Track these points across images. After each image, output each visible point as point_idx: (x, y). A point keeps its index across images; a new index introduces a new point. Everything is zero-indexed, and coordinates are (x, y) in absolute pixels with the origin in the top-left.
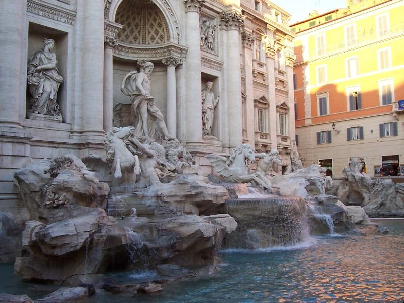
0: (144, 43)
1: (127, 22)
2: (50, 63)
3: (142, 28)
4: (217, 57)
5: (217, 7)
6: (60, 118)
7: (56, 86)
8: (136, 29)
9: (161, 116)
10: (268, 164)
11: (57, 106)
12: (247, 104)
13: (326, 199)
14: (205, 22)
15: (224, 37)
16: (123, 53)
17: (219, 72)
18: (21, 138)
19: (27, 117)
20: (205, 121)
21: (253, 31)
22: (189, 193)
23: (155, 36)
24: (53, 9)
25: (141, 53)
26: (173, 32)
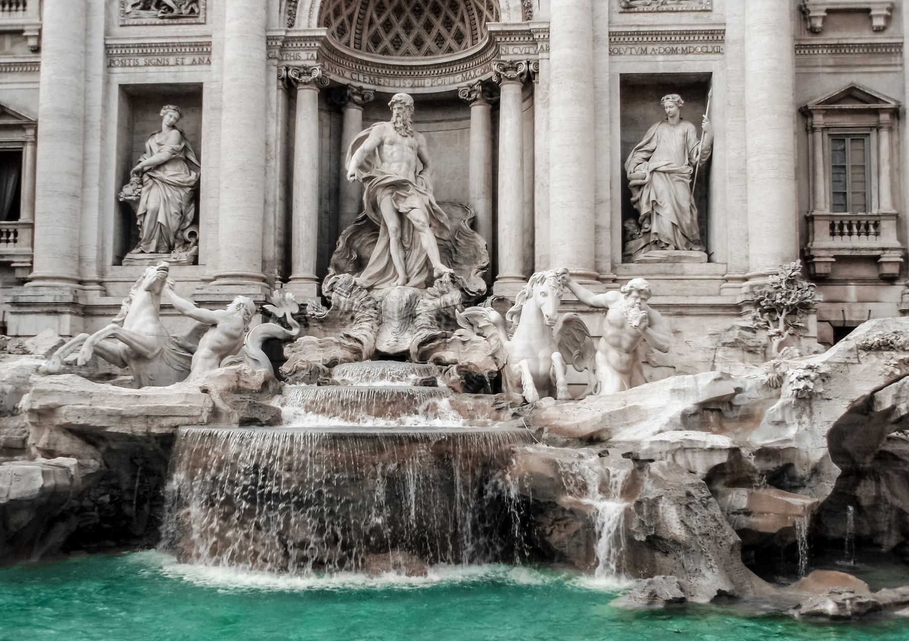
1: (429, 6)
2: (159, 151)
3: (465, 11)
4: (706, 15)
7: (179, 196)
8: (456, 14)
9: (418, 221)
10: (622, 326)
13: (667, 448)
16: (428, 82)
17: (713, 56)
18: (48, 304)
19: (119, 261)
20: (645, 210)
23: (489, 16)
24: (162, 45)
25: (466, 70)
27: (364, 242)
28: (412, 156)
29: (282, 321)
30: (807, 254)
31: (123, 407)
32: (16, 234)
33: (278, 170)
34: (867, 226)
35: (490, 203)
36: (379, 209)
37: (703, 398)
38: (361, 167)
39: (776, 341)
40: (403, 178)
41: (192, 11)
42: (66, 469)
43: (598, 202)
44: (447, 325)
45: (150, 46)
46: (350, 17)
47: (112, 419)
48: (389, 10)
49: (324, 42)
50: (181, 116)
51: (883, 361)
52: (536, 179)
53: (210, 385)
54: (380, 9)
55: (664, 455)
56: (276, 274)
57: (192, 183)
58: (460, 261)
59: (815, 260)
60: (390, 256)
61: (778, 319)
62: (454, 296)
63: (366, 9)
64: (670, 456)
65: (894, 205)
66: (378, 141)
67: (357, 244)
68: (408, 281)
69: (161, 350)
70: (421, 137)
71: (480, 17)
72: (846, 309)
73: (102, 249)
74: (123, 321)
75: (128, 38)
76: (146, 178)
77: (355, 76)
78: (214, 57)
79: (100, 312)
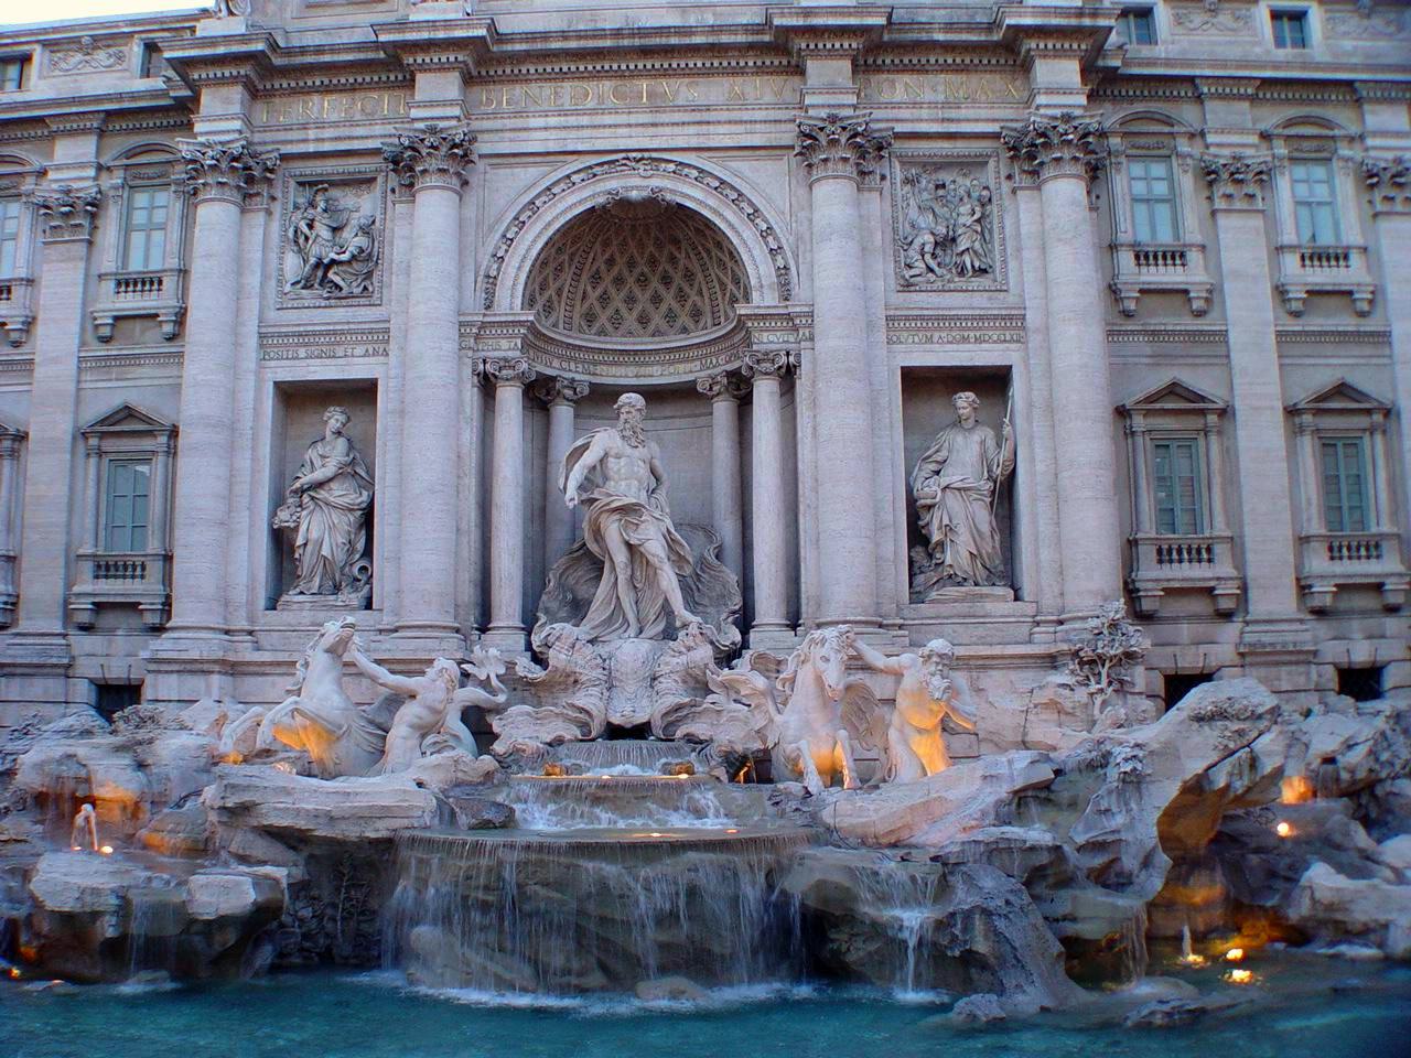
0: (716, 321)
3: (703, 282)
5: (977, 120)
6: (355, 599)
7: (345, 523)
11: (363, 569)
12: (1242, 434)
14: (943, 186)
15: (1021, 215)
16: (656, 370)
19: (272, 605)
20: (936, 537)
21: (1266, 137)
22: (221, 804)
25: (706, 356)
26: (758, 266)
27: (581, 577)
28: (643, 471)
29: (485, 684)
30: (1131, 587)
31: (328, 805)
32: (143, 568)
33: (474, 489)
34: (1199, 551)
35: (739, 525)
36: (603, 539)
37: (1019, 785)
38: (581, 488)
39: (1099, 699)
40: (634, 501)
41: (365, 288)
42: (276, 881)
43: (878, 528)
44: (694, 689)
45: (314, 334)
46: (559, 292)
47: (320, 821)
48: (608, 280)
49: (532, 327)
50: (349, 419)
51: (1216, 733)
52: (801, 499)
53: (424, 777)
54: (596, 278)
55: (978, 857)
56: (472, 620)
57: (364, 505)
58: (706, 601)
59: (1141, 594)
60: (618, 598)
61: (1099, 674)
62: (704, 653)
63: (578, 281)
64: (984, 859)
65: (1228, 525)
66: (602, 454)
67: (571, 581)
68: (641, 632)
69: (349, 727)
70: (654, 446)
71: (724, 290)
72: (1178, 654)
73: (251, 589)
74: (300, 689)
75: (288, 325)
76: (306, 498)
77: (565, 365)
78: (393, 347)
79: (256, 669)
